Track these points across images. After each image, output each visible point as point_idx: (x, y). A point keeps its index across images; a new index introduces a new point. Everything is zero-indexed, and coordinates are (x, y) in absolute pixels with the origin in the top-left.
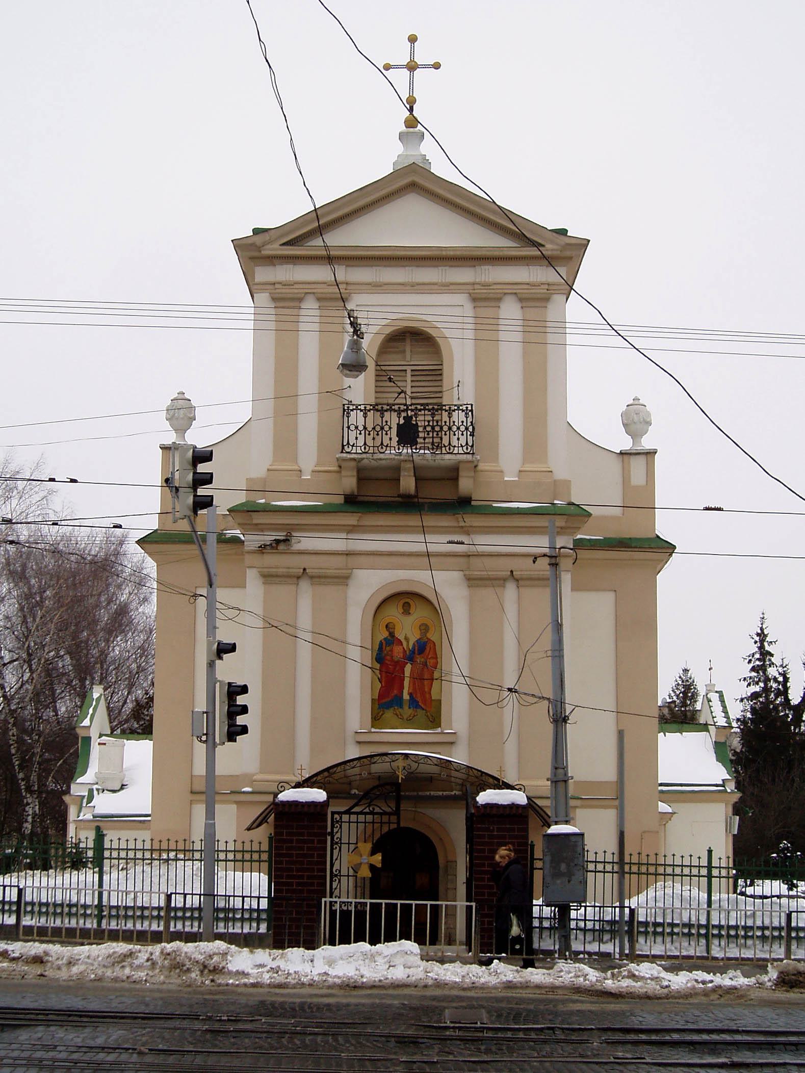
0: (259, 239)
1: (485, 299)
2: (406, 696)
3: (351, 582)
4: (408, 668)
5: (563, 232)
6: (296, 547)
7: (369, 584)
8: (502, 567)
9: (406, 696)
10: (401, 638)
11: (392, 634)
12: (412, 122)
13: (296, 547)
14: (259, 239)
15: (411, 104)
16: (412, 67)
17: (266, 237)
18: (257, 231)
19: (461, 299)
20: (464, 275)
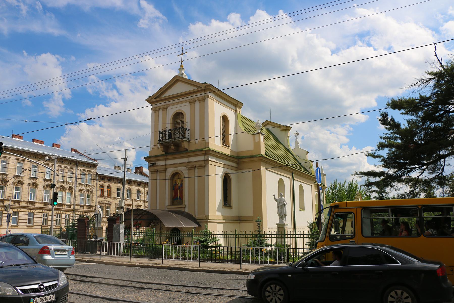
0: (150, 99)
1: (192, 102)
5: (205, 83)
11: (176, 183)
12: (181, 66)
15: (182, 61)
16: (182, 54)
17: (151, 98)
18: (149, 97)
19: (188, 103)
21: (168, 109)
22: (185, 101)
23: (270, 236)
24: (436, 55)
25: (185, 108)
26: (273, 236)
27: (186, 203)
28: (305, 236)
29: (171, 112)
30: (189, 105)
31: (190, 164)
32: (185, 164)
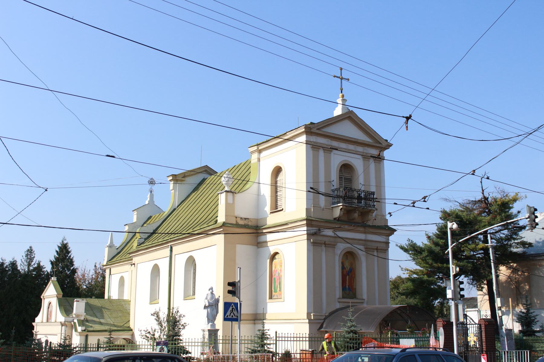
0: (312, 126)
1: (366, 157)
2: (347, 287)
3: (336, 246)
4: (347, 277)
6: (321, 234)
7: (342, 247)
8: (375, 245)
9: (347, 287)
10: (345, 267)
13: (321, 234)
14: (312, 126)
16: (342, 79)
18: (312, 123)
19: (360, 157)
20: (360, 149)
21: (332, 154)
22: (356, 153)
23: (190, 344)
24: (481, 182)
25: (357, 163)
26: (196, 344)
27: (365, 297)
28: (196, 344)
29: (338, 159)
30: (362, 159)
31: (369, 244)
32: (361, 242)
